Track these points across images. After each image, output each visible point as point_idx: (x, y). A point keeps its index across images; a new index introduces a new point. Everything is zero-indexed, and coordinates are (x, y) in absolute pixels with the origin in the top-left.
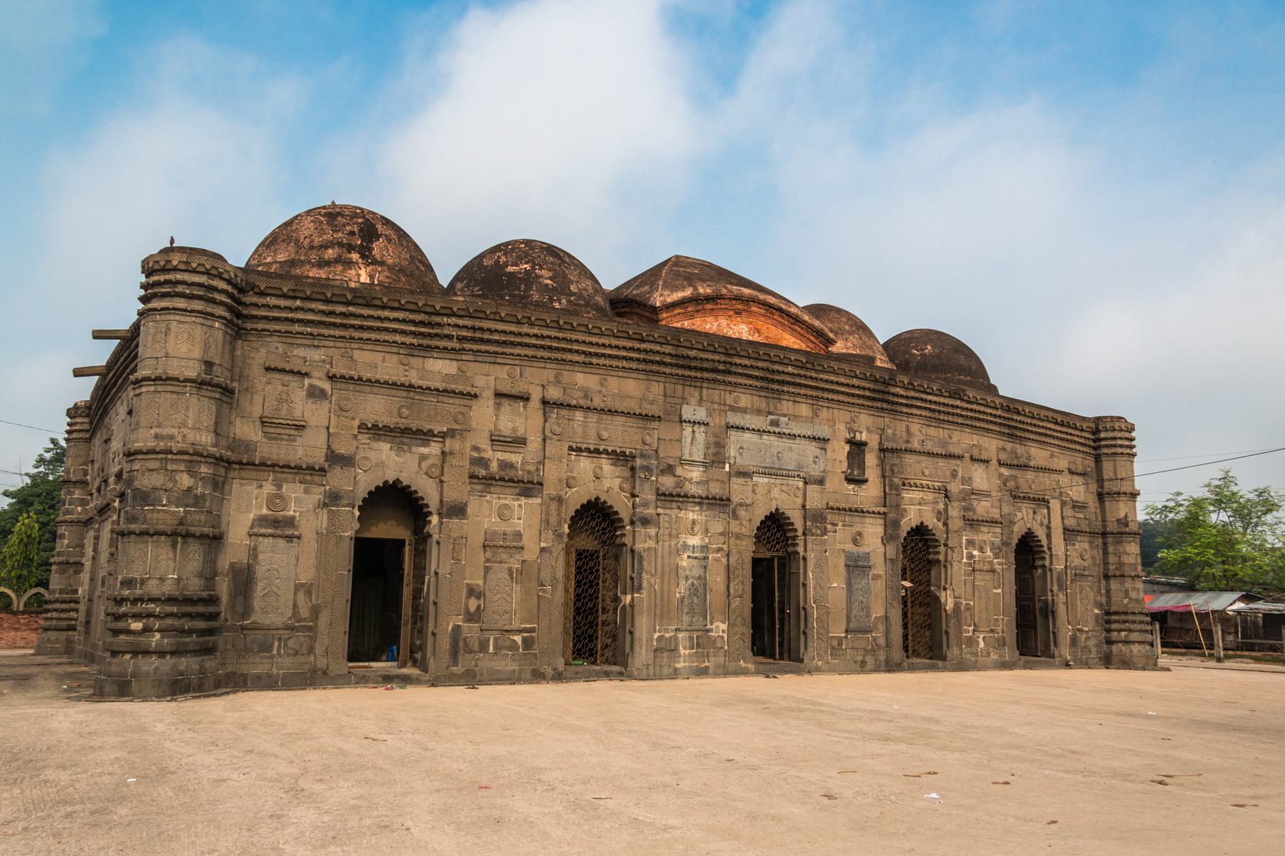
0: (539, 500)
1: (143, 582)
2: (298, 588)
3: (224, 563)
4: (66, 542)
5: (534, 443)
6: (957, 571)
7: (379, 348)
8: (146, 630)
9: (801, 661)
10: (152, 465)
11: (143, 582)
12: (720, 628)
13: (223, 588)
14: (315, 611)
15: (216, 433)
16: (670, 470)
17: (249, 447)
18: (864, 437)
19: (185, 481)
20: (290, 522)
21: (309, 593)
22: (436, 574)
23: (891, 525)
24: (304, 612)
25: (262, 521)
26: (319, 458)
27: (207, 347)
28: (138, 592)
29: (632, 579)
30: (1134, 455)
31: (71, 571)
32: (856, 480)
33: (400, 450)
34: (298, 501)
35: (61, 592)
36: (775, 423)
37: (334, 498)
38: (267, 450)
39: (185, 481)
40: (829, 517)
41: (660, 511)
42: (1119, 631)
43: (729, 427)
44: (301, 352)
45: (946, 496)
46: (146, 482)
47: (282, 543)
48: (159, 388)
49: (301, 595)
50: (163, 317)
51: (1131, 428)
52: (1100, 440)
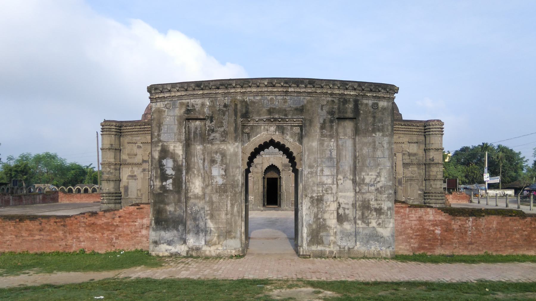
2: (138, 190)
3: (122, 185)
8: (103, 199)
13: (122, 190)
14: (142, 194)
15: (115, 158)
17: (125, 160)
19: (108, 169)
20: (135, 176)
21: (140, 191)
24: (139, 195)
25: (129, 176)
26: (141, 161)
27: (111, 141)
34: (137, 171)
37: (144, 170)
38: (129, 161)
39: (108, 169)
44: (135, 138)
47: (134, 180)
49: (138, 192)
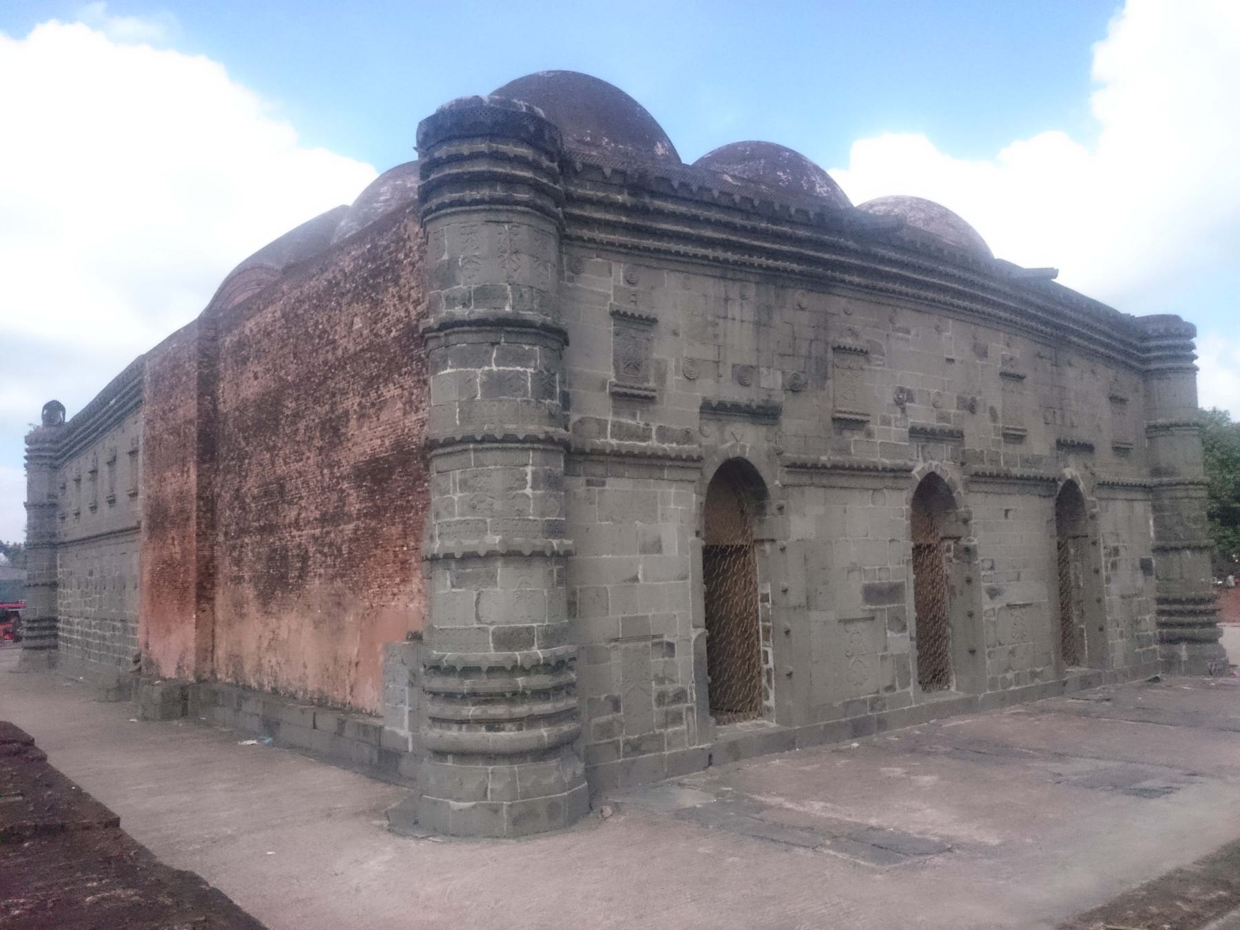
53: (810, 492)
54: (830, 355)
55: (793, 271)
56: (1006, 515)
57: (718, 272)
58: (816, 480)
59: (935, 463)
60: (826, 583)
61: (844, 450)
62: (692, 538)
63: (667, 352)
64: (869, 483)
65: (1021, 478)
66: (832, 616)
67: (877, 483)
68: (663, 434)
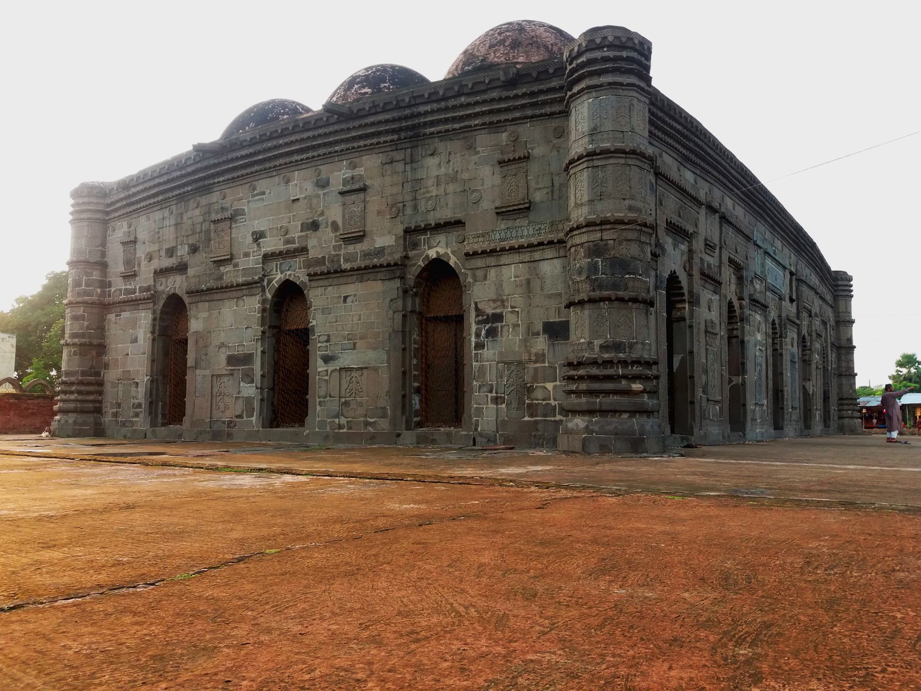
0: (717, 297)
1: (631, 346)
4: (86, 323)
5: (717, 251)
6: (814, 366)
7: (672, 153)
9: (782, 428)
10: (631, 235)
11: (631, 346)
12: (765, 402)
16: (752, 282)
18: (793, 269)
22: (691, 352)
23: (799, 334)
28: (633, 356)
29: (743, 364)
30: (852, 296)
31: (94, 353)
32: (792, 300)
33: (675, 246)
35: (84, 373)
36: (775, 253)
40: (788, 326)
41: (751, 313)
42: (847, 410)
43: (766, 253)
45: (810, 316)
46: (624, 252)
48: (630, 162)
50: (626, 93)
51: (850, 279)
52: (838, 286)
53: (200, 305)
54: (212, 226)
55: (188, 191)
56: (345, 301)
57: (159, 207)
58: (203, 298)
59: (289, 273)
60: (206, 354)
61: (220, 278)
62: (149, 335)
63: (141, 252)
64: (234, 294)
65: (352, 270)
66: (208, 372)
67: (239, 294)
68: (142, 290)
